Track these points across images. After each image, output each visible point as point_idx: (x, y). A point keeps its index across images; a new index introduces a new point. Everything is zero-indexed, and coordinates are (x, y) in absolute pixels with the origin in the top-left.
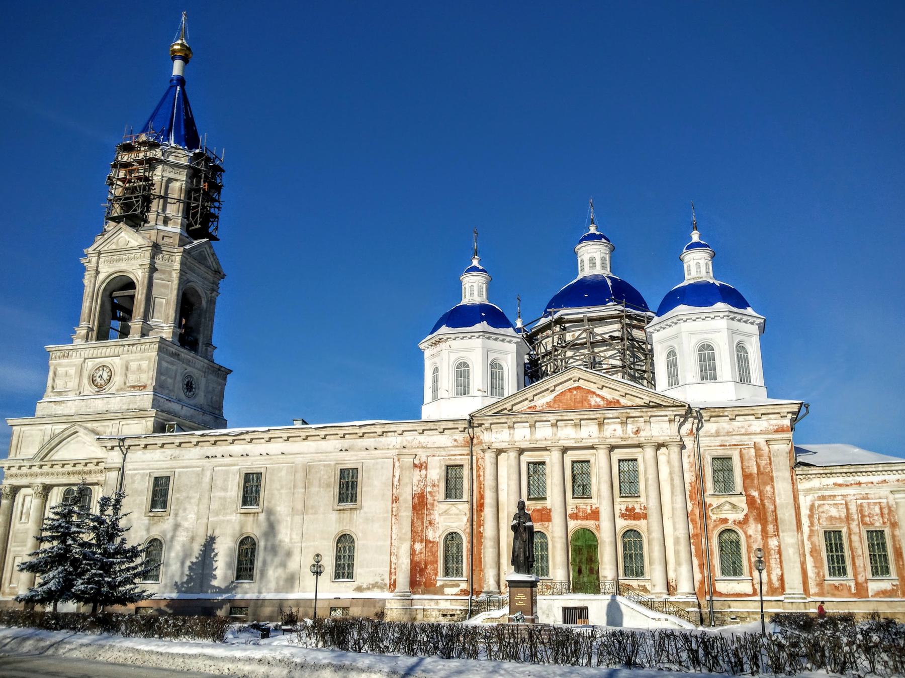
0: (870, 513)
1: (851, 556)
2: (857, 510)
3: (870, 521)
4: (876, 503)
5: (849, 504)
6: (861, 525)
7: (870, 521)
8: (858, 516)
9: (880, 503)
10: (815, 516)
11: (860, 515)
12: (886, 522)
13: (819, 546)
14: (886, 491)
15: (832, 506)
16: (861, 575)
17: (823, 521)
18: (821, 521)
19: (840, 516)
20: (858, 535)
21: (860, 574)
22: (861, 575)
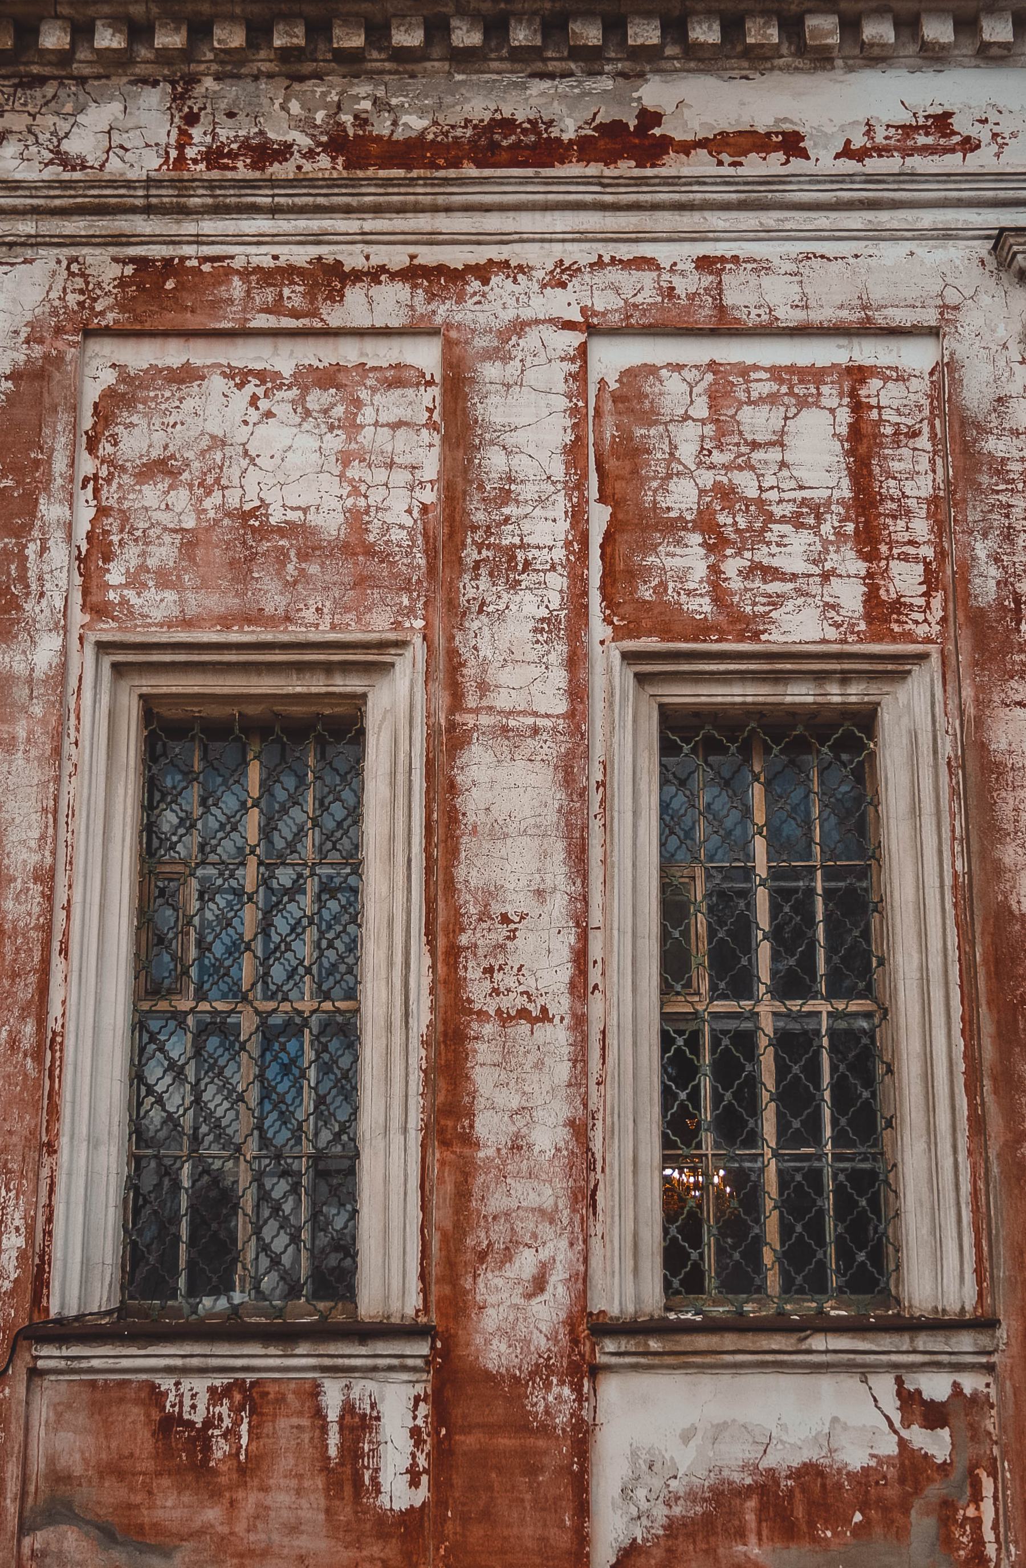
0: (727, 494)
1: (423, 1017)
2: (574, 452)
3: (718, 594)
4: (815, 375)
5: (491, 371)
6: (599, 629)
7: (718, 594)
8: (578, 516)
9: (858, 374)
10: (51, 511)
11: (599, 517)
12: (898, 606)
13: (45, 877)
14: (947, 234)
15: (282, 403)
16: (526, 1263)
17: (135, 581)
18: (115, 576)
19: (357, 519)
20: (550, 749)
21: (507, 1256)
22: (526, 1263)
